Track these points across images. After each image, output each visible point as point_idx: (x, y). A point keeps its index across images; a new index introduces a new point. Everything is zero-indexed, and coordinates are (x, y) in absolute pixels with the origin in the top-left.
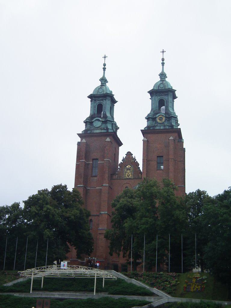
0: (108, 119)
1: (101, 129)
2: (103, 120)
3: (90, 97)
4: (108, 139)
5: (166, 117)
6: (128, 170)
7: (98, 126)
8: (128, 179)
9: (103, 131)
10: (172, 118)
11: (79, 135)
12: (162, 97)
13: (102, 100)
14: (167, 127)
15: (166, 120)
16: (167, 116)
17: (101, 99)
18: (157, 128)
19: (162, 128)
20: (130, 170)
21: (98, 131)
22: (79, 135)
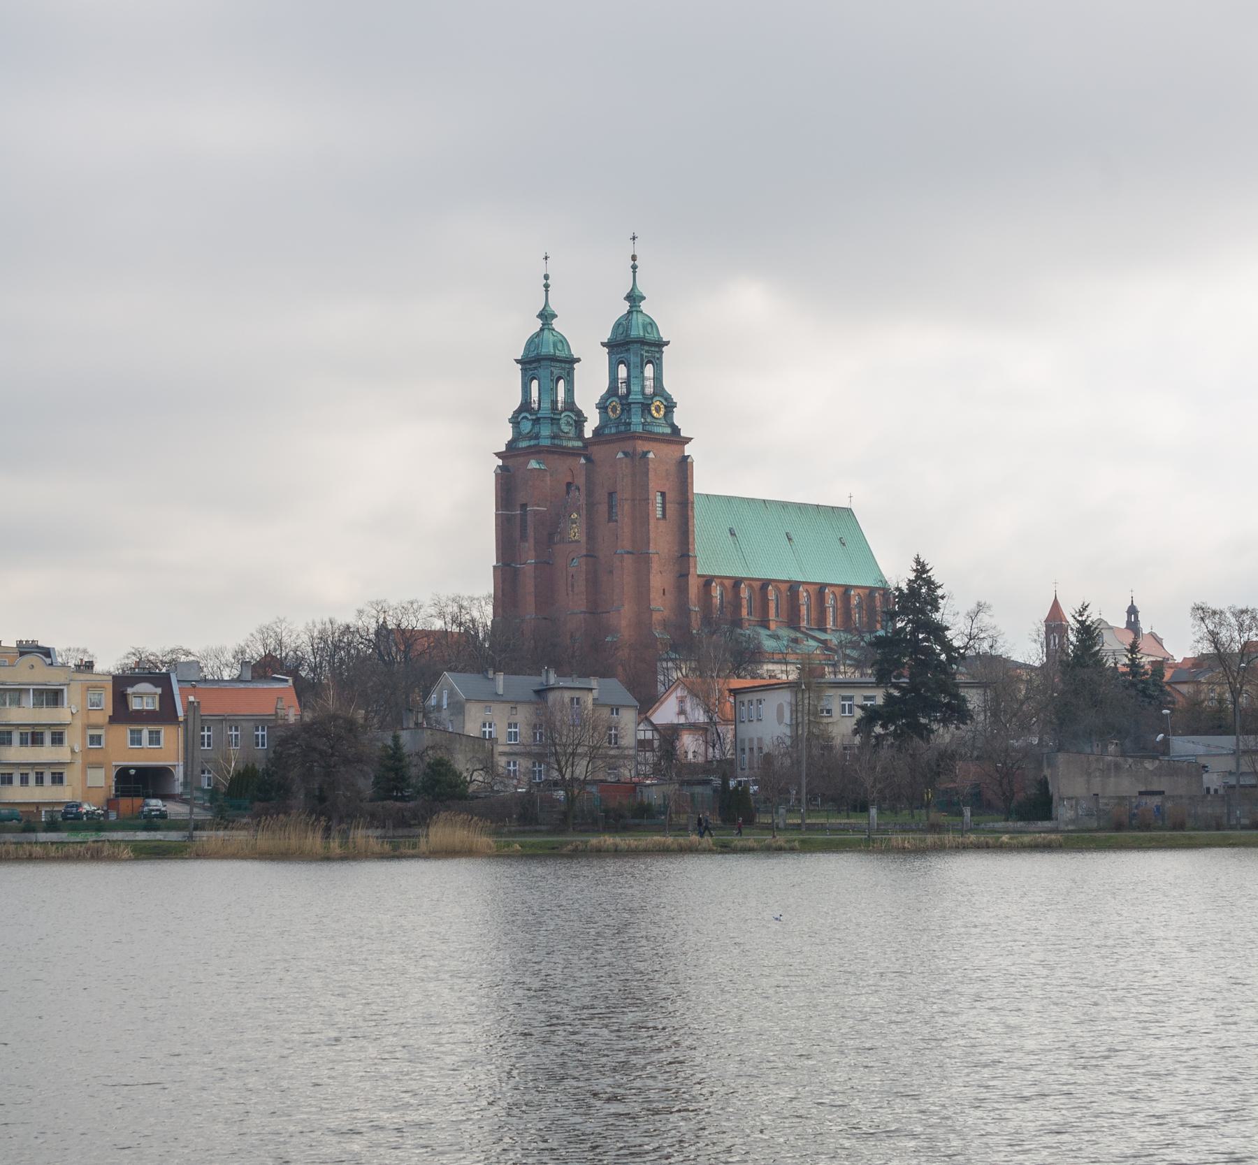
0: (539, 416)
1: (531, 439)
2: (534, 417)
3: (518, 361)
4: (533, 464)
5: (622, 404)
6: (573, 523)
7: (527, 431)
8: (573, 542)
9: (532, 443)
10: (632, 405)
11: (498, 455)
12: (622, 355)
13: (535, 368)
14: (622, 428)
15: (622, 410)
16: (624, 402)
17: (534, 365)
18: (607, 431)
19: (613, 430)
20: (576, 523)
21: (523, 444)
22: (498, 455)
